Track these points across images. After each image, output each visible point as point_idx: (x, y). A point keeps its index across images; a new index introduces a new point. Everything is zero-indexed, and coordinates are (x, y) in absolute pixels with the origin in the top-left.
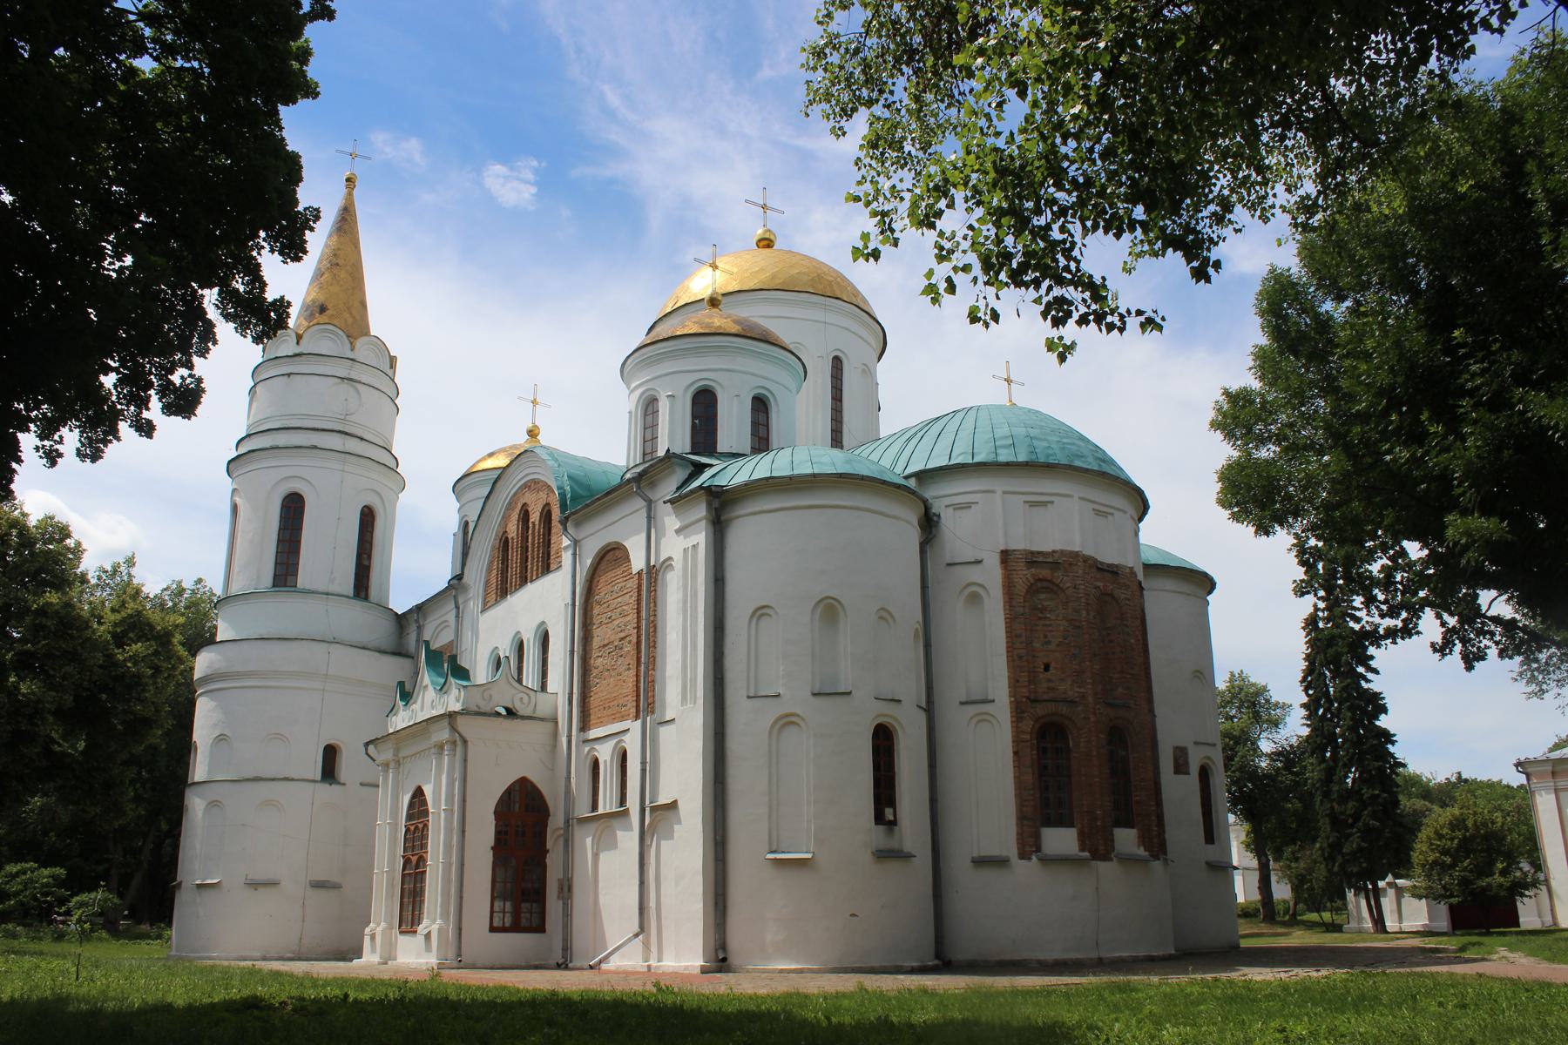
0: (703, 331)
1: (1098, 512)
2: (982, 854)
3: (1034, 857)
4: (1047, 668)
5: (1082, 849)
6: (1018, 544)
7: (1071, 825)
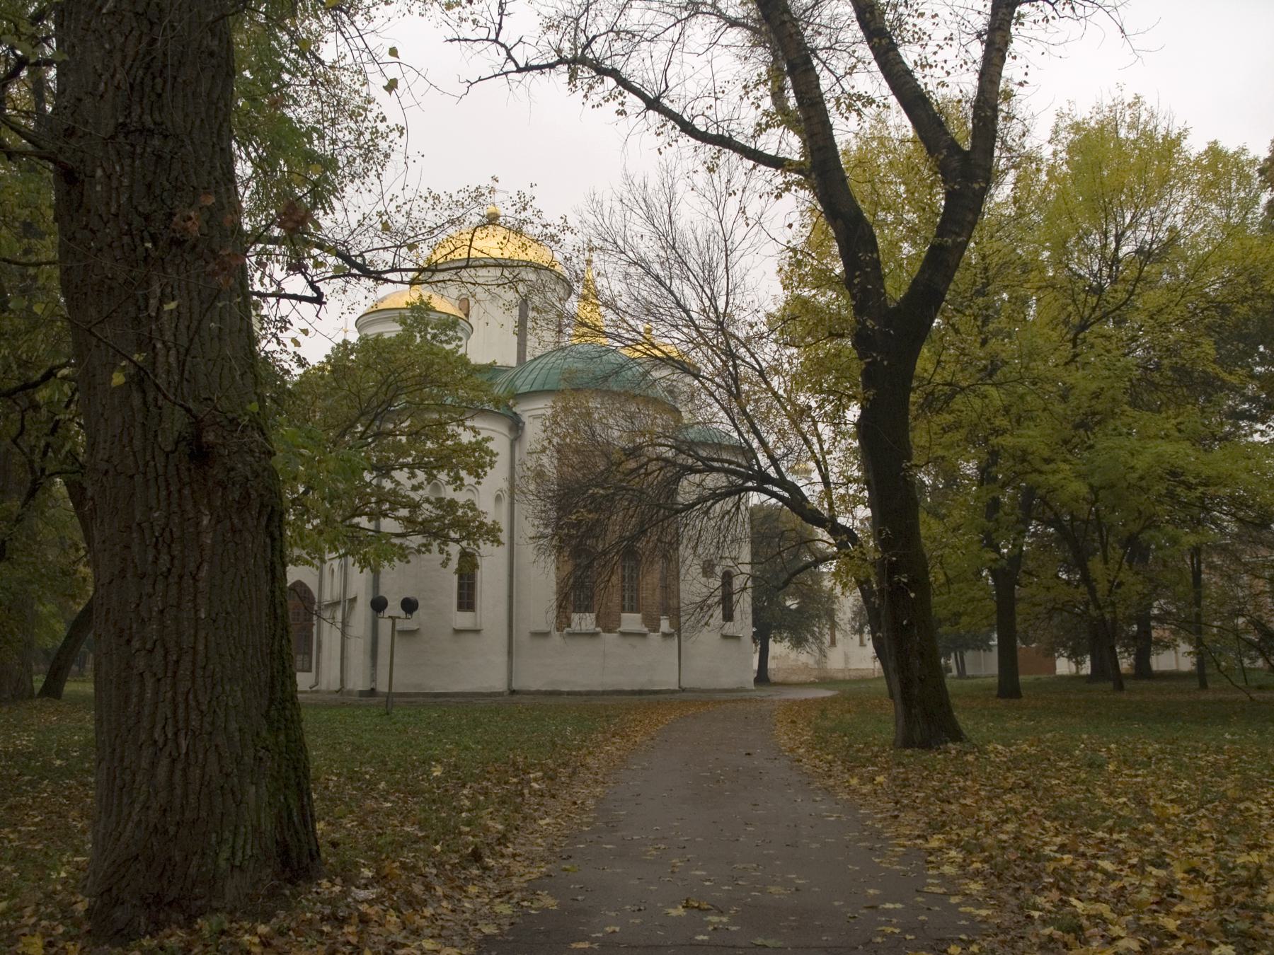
5: (597, 625)
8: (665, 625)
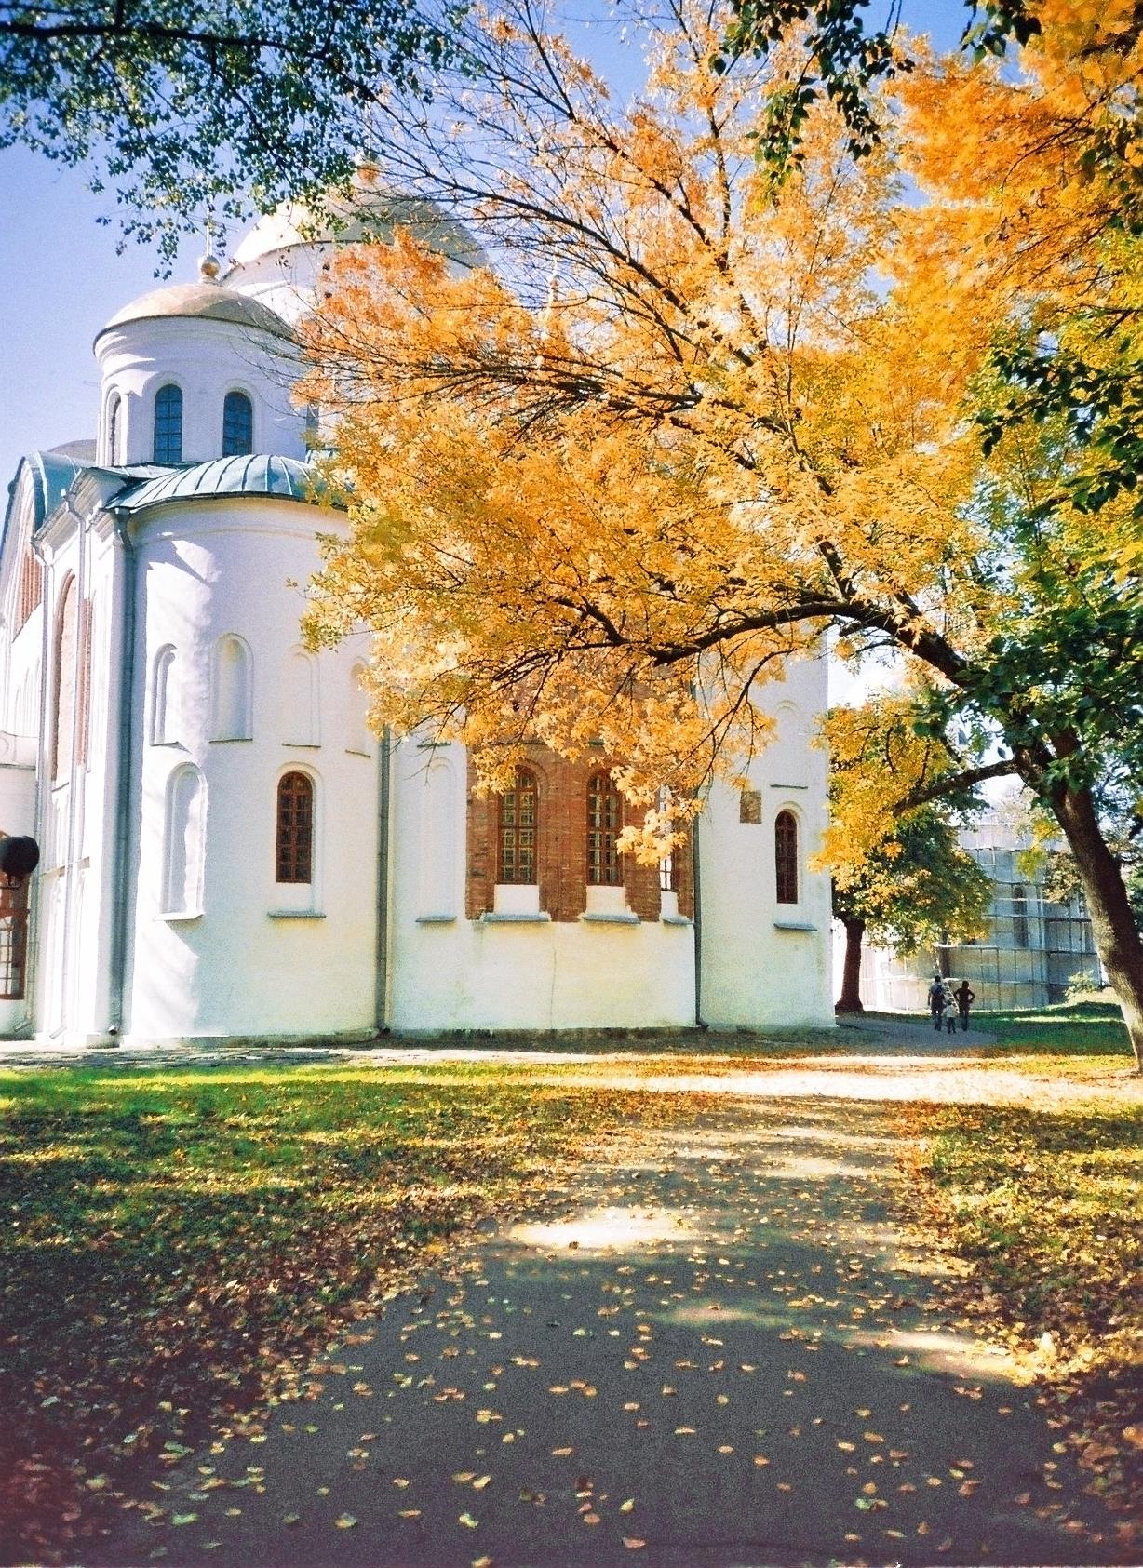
5: (544, 907)
7: (535, 883)
8: (669, 902)
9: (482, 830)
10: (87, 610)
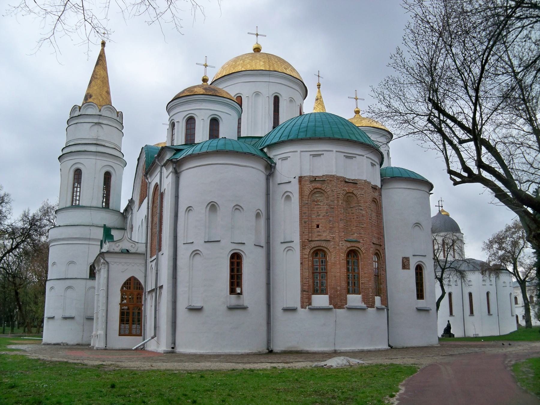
0: (189, 94)
1: (347, 157)
2: (288, 306)
3: (307, 307)
4: (318, 226)
5: (330, 304)
6: (306, 173)
7: (327, 294)
9: (307, 274)
10: (162, 195)
